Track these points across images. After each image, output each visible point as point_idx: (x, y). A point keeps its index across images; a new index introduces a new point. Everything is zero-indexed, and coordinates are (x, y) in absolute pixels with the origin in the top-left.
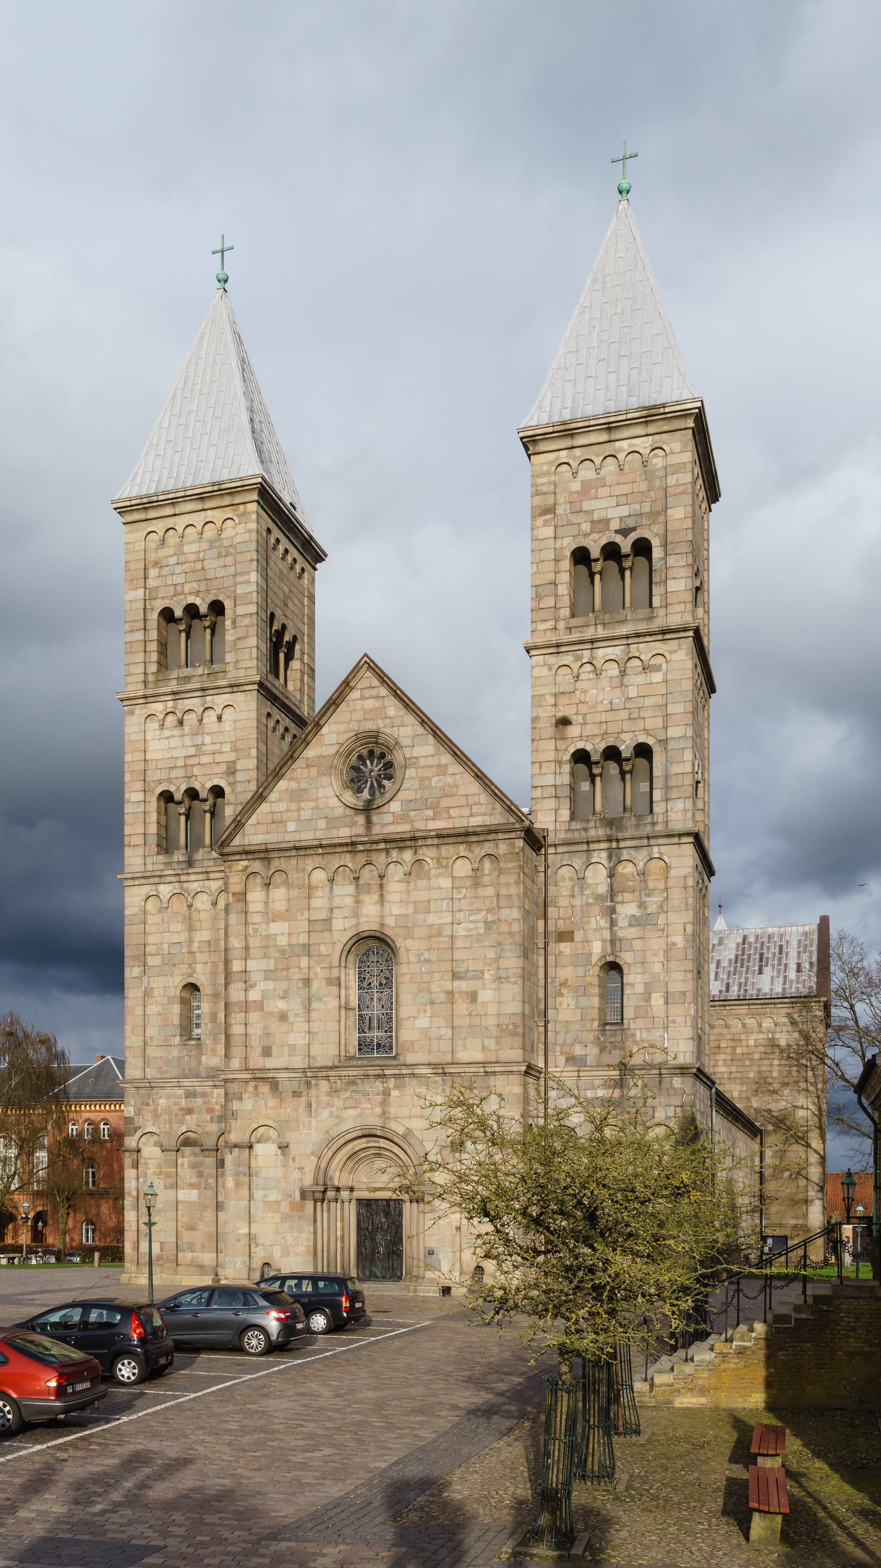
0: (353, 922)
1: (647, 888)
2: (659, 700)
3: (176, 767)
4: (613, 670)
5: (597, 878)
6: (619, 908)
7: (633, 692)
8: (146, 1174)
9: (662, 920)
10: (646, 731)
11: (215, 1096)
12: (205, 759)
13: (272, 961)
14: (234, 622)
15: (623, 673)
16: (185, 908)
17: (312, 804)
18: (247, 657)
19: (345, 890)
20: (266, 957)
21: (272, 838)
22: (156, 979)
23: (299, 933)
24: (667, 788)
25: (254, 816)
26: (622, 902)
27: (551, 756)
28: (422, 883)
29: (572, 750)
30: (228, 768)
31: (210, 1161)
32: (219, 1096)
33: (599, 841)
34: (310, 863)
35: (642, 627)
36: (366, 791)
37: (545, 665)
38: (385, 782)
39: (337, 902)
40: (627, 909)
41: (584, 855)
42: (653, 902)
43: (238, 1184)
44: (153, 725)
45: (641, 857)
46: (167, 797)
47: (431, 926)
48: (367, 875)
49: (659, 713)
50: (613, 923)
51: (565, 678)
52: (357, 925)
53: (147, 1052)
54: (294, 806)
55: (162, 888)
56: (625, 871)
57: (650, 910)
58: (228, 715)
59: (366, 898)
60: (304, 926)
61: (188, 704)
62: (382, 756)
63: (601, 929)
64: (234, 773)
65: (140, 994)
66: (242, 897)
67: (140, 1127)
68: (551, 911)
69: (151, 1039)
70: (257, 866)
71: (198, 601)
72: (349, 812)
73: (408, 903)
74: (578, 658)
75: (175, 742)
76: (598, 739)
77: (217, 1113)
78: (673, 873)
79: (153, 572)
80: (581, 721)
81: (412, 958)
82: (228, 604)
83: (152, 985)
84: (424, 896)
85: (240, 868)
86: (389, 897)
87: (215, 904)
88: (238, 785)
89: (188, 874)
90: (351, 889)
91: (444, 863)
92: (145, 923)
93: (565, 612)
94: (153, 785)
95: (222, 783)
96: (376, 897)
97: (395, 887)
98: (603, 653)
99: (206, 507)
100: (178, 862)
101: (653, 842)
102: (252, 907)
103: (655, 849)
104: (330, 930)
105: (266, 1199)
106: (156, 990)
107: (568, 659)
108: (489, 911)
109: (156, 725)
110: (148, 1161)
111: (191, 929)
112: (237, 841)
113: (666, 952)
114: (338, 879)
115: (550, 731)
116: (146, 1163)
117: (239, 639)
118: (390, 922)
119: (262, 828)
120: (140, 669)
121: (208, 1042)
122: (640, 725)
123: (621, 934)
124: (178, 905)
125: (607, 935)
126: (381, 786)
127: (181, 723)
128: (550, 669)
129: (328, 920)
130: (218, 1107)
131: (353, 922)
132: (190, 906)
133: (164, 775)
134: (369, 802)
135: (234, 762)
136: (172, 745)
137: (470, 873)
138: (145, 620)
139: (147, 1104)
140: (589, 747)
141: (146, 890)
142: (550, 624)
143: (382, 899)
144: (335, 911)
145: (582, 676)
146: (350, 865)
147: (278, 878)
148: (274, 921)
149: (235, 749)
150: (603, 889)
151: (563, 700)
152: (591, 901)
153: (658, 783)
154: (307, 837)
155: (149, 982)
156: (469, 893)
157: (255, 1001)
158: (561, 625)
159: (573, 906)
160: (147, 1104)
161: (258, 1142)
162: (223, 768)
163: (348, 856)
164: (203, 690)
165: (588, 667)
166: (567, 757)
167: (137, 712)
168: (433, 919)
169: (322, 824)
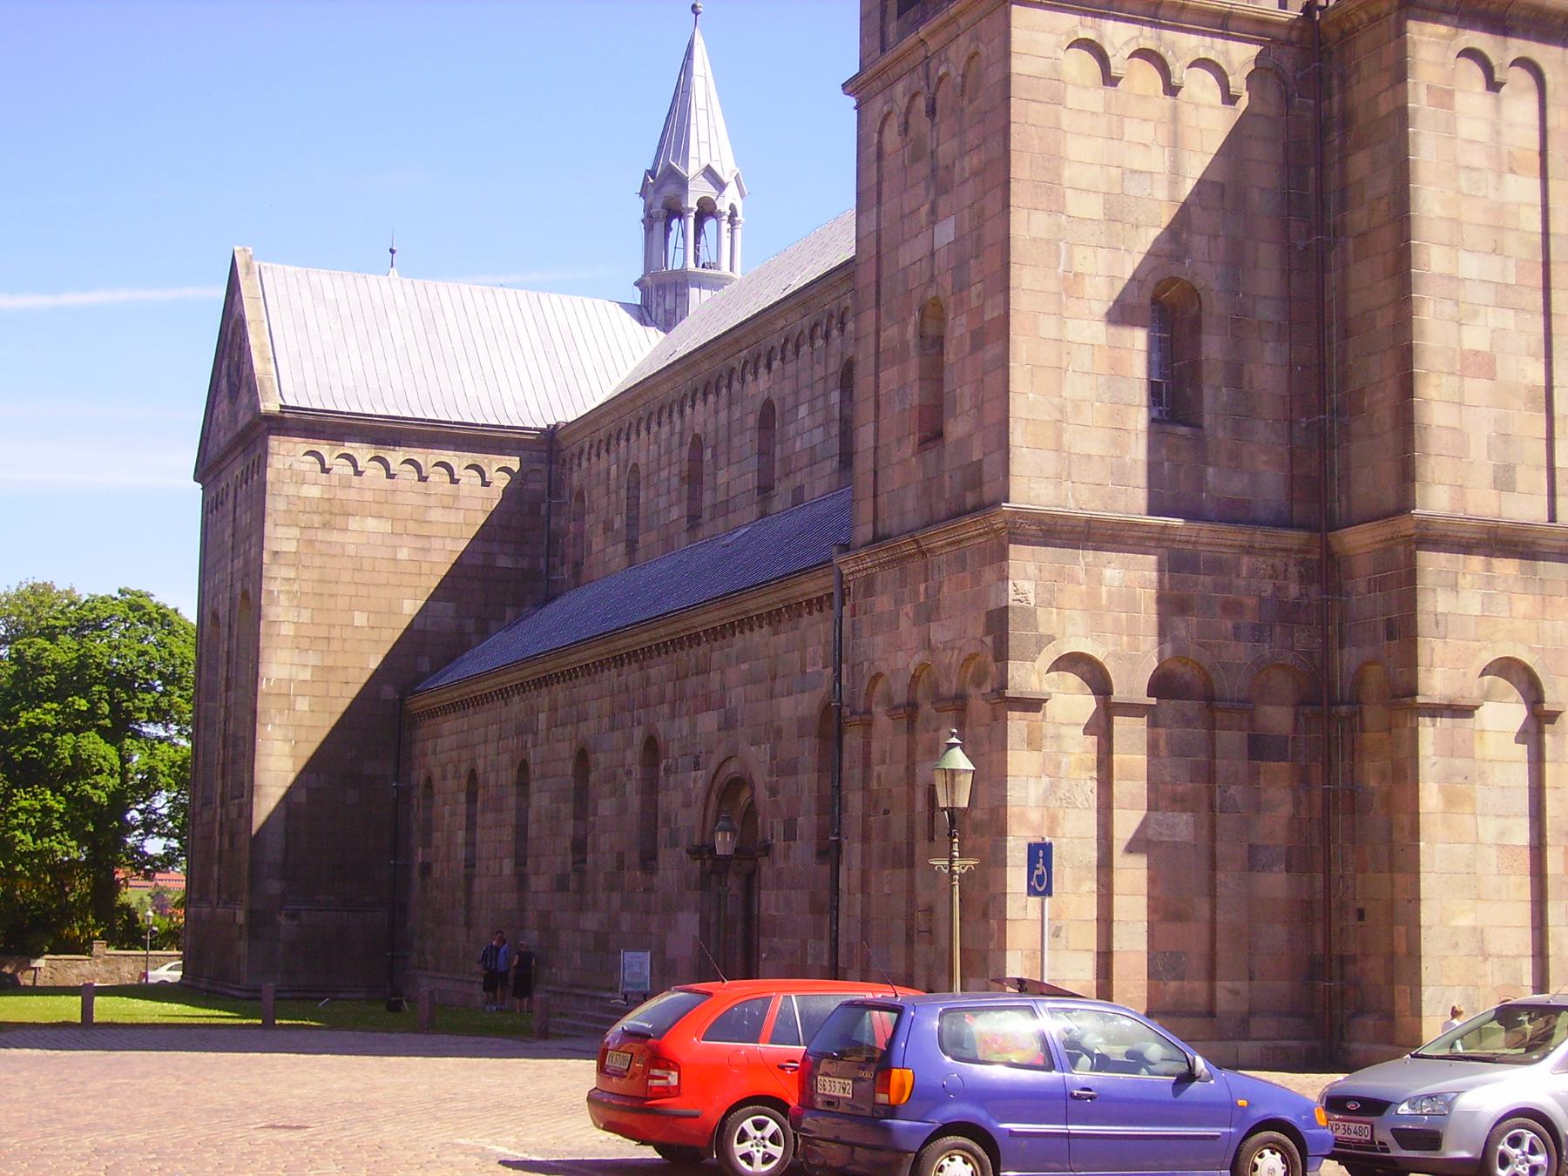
8: (1058, 766)
11: (1244, 571)
13: (1511, 264)
20: (1496, 250)
22: (1089, 252)
31: (1231, 740)
32: (1253, 573)
43: (1451, 801)
53: (1066, 438)
65: (1052, 286)
67: (1052, 638)
69: (1077, 407)
77: (1249, 618)
83: (1079, 269)
105: (1505, 842)
106: (1087, 280)
110: (1064, 730)
116: (1057, 737)
121: (1221, 434)
130: (1250, 602)
139: (1073, 579)
148: (1512, 171)
155: (1070, 257)
157: (1476, 353)
160: (1073, 579)
161: (1487, 697)
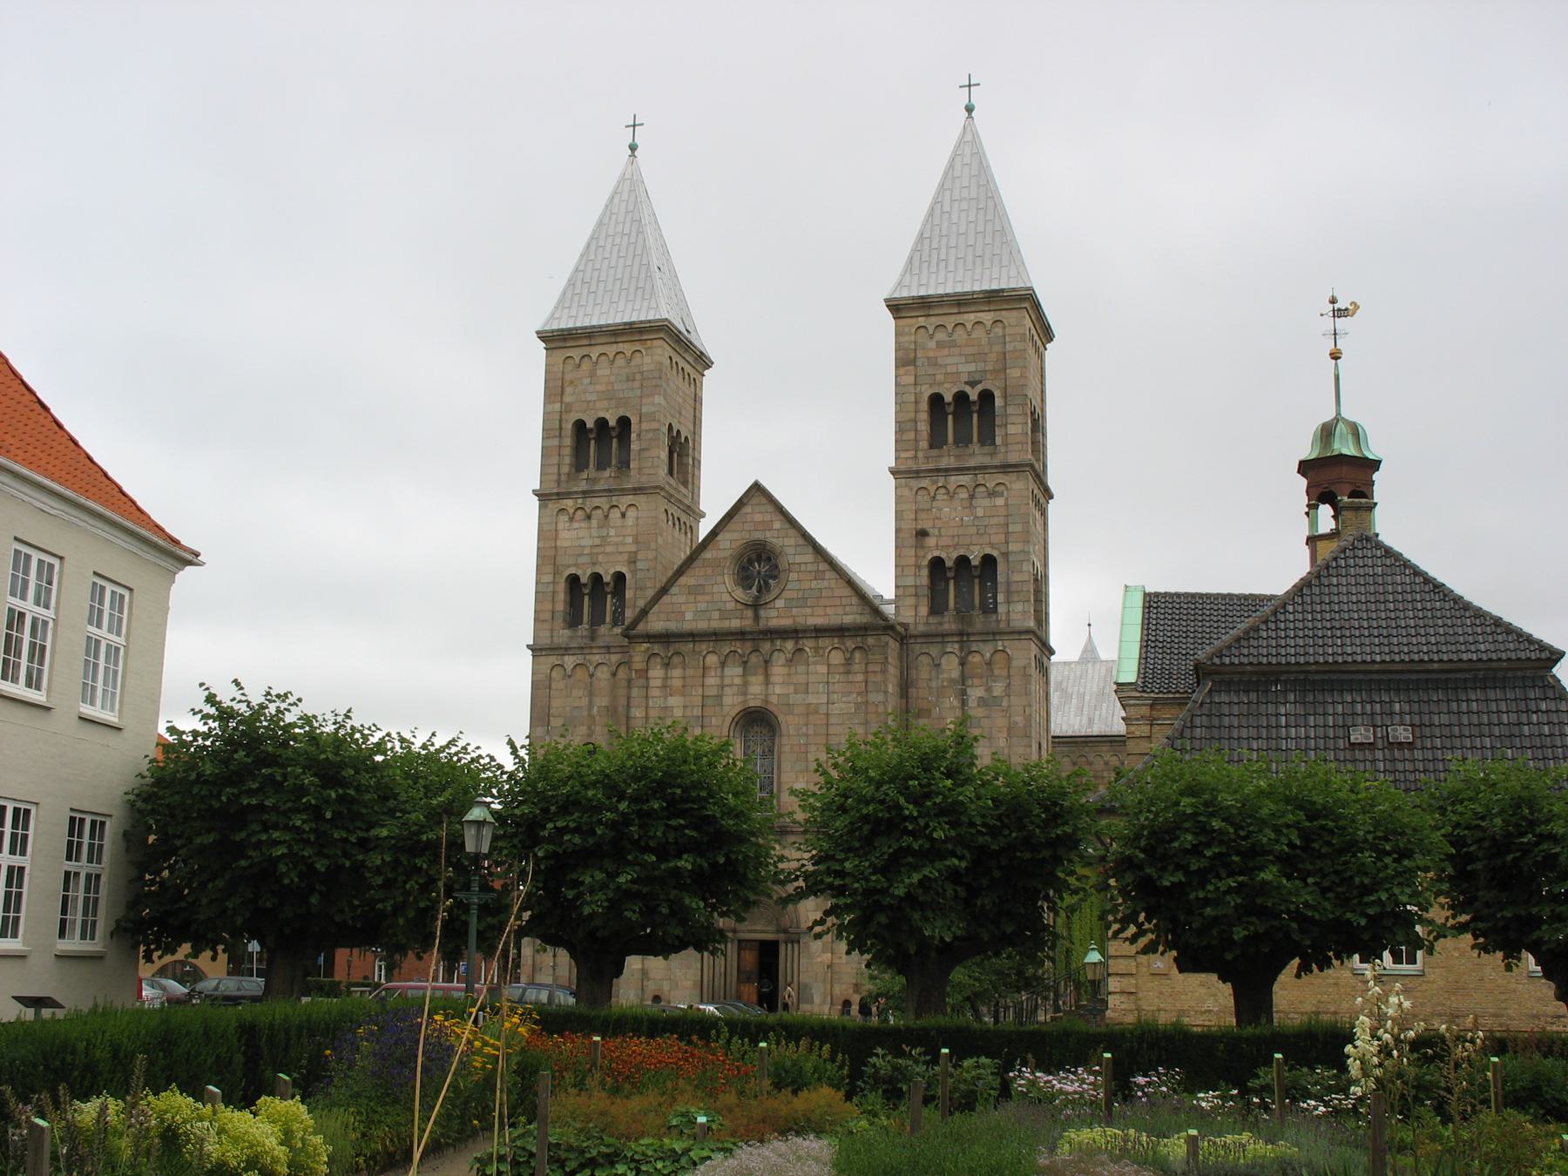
0: (741, 699)
1: (992, 675)
2: (1002, 520)
3: (581, 555)
4: (964, 494)
5: (951, 666)
6: (969, 691)
7: (980, 512)
9: (1005, 703)
10: (991, 545)
12: (609, 549)
14: (639, 435)
15: (972, 497)
16: (587, 677)
17: (707, 598)
18: (650, 464)
19: (734, 672)
21: (673, 626)
23: (693, 706)
24: (1008, 593)
25: (657, 606)
26: (972, 686)
27: (912, 561)
28: (801, 668)
29: (930, 557)
30: (630, 557)
33: (952, 635)
34: (703, 647)
35: (986, 461)
36: (754, 588)
37: (907, 486)
38: (771, 581)
39: (727, 682)
40: (975, 693)
41: (939, 646)
42: (998, 689)
44: (564, 518)
45: (988, 650)
46: (573, 581)
47: (809, 704)
48: (754, 659)
49: (1001, 530)
50: (964, 703)
51: (923, 498)
52: (745, 701)
54: (691, 598)
55: (566, 658)
56: (974, 660)
57: (995, 694)
58: (631, 513)
59: (752, 679)
60: (698, 701)
61: (597, 501)
62: (769, 559)
63: (954, 708)
64: (635, 562)
66: (644, 673)
68: (912, 691)
70: (657, 648)
71: (607, 416)
72: (739, 606)
73: (788, 684)
74: (934, 483)
75: (582, 533)
76: (951, 549)
78: (1015, 663)
79: (568, 390)
80: (937, 533)
81: (792, 732)
82: (634, 420)
84: (802, 679)
85: (643, 649)
86: (773, 679)
87: (614, 674)
88: (638, 573)
89: (591, 647)
90: (740, 670)
91: (821, 652)
92: (550, 688)
93: (924, 444)
94: (561, 569)
95: (624, 570)
96: (761, 678)
97: (778, 670)
98: (954, 480)
99: (618, 340)
100: (582, 637)
101: (997, 637)
102: (652, 683)
103: (1000, 643)
104: (721, 705)
107: (925, 483)
108: (859, 694)
109: (566, 518)
111: (591, 694)
112: (641, 627)
113: (1008, 729)
114: (729, 661)
115: (911, 541)
117: (644, 449)
118: (774, 699)
119: (663, 616)
120: (555, 470)
122: (986, 539)
123: (971, 713)
124: (580, 674)
125: (959, 713)
126: (766, 583)
127: (589, 517)
128: (911, 490)
129: (720, 697)
131: (741, 699)
132: (591, 676)
133: (572, 561)
134: (757, 598)
135: (636, 553)
136: (581, 535)
137: (843, 662)
138: (561, 428)
140: (943, 555)
141: (554, 660)
142: (911, 454)
143: (767, 683)
144: (725, 689)
145: (938, 497)
146: (739, 651)
147: (676, 660)
148: (671, 695)
149: (636, 541)
150: (955, 674)
151: (922, 515)
152: (945, 684)
153: (1001, 588)
154: (702, 625)
156: (842, 678)
158: (920, 454)
159: (930, 688)
162: (626, 557)
163: (738, 644)
164: (610, 490)
165: (942, 491)
166: (925, 562)
167: (550, 506)
168: (812, 699)
169: (716, 615)
